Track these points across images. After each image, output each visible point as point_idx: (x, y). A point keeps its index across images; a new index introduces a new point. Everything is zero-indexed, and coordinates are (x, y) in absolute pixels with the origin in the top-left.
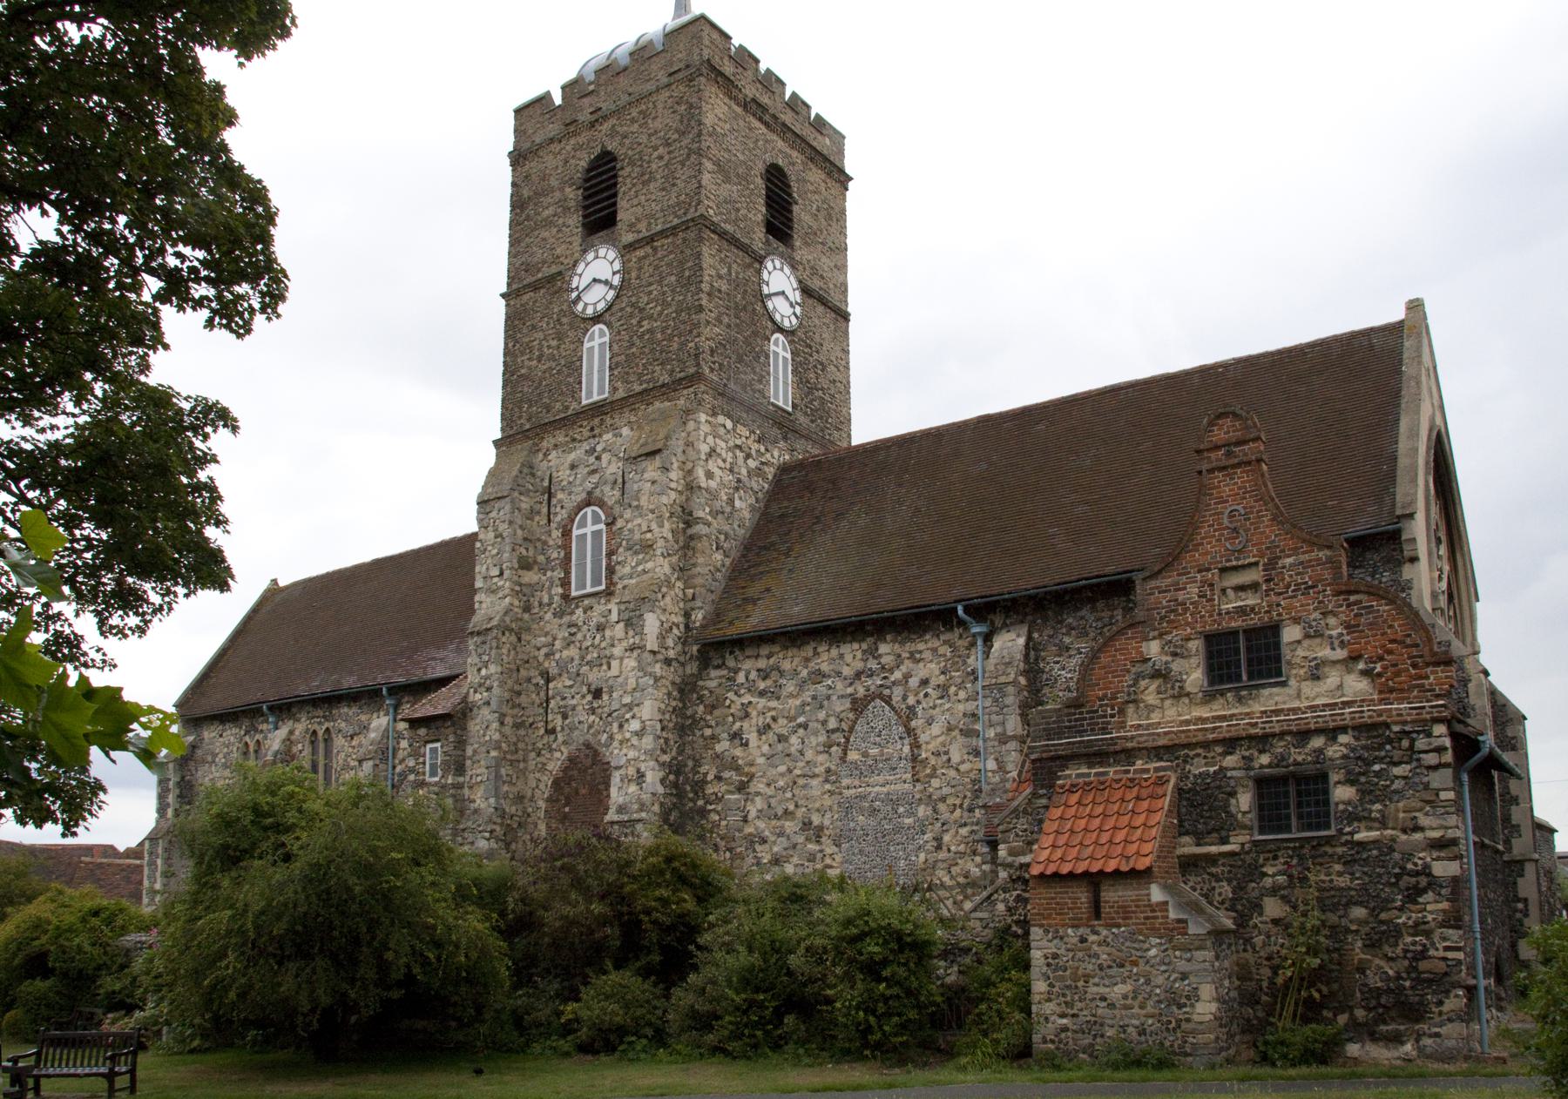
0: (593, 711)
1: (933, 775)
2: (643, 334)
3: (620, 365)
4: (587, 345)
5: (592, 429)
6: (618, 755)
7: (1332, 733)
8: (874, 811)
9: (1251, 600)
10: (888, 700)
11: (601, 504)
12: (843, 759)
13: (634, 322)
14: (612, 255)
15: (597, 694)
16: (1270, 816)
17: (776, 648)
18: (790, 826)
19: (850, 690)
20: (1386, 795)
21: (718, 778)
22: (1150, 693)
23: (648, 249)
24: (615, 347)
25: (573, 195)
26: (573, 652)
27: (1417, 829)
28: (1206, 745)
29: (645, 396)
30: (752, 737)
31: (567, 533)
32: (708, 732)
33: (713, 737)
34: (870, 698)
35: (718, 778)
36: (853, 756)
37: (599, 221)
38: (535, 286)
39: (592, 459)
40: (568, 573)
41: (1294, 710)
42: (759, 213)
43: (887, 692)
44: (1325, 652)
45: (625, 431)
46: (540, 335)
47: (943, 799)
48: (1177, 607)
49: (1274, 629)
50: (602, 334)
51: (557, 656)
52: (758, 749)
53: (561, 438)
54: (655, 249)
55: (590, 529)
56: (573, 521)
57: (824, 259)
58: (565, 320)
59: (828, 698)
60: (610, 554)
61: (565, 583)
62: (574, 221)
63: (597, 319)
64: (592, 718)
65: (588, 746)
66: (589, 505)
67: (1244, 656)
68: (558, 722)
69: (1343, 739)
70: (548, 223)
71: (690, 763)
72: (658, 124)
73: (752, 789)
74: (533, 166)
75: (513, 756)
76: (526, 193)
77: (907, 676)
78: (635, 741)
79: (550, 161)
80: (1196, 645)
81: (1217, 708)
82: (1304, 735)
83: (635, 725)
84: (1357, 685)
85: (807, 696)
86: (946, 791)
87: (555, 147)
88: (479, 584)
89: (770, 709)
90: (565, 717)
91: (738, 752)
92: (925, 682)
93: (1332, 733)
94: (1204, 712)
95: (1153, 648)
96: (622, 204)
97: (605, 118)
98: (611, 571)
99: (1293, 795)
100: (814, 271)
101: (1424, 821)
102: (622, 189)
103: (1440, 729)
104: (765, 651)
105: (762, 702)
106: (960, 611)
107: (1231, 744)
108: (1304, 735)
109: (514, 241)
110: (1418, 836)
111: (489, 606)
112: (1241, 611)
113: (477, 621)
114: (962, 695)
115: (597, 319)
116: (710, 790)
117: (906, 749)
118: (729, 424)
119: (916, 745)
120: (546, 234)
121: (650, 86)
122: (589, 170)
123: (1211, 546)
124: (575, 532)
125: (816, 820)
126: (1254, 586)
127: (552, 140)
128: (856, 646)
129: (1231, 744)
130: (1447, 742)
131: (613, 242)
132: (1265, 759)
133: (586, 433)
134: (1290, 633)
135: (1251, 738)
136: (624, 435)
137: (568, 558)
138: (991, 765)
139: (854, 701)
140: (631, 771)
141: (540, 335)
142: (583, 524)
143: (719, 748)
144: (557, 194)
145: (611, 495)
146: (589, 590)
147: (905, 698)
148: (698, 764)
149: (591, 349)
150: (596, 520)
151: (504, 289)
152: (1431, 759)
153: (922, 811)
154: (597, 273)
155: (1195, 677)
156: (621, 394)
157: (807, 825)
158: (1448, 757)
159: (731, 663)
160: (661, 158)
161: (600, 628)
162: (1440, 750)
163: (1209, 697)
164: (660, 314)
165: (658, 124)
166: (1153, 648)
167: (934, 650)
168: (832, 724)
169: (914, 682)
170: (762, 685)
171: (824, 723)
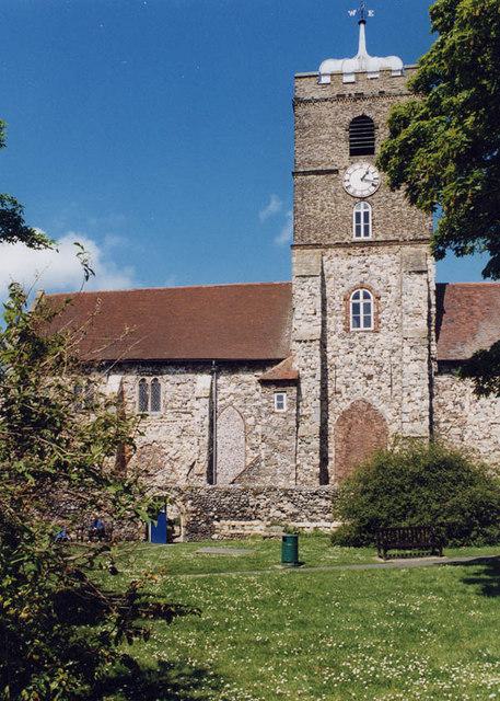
24: (376, 215)
30: (466, 404)
35: (448, 421)
51: (341, 357)
53: (340, 251)
62: (345, 146)
64: (366, 389)
68: (343, 388)
70: (323, 142)
122: (351, 123)
144: (331, 130)
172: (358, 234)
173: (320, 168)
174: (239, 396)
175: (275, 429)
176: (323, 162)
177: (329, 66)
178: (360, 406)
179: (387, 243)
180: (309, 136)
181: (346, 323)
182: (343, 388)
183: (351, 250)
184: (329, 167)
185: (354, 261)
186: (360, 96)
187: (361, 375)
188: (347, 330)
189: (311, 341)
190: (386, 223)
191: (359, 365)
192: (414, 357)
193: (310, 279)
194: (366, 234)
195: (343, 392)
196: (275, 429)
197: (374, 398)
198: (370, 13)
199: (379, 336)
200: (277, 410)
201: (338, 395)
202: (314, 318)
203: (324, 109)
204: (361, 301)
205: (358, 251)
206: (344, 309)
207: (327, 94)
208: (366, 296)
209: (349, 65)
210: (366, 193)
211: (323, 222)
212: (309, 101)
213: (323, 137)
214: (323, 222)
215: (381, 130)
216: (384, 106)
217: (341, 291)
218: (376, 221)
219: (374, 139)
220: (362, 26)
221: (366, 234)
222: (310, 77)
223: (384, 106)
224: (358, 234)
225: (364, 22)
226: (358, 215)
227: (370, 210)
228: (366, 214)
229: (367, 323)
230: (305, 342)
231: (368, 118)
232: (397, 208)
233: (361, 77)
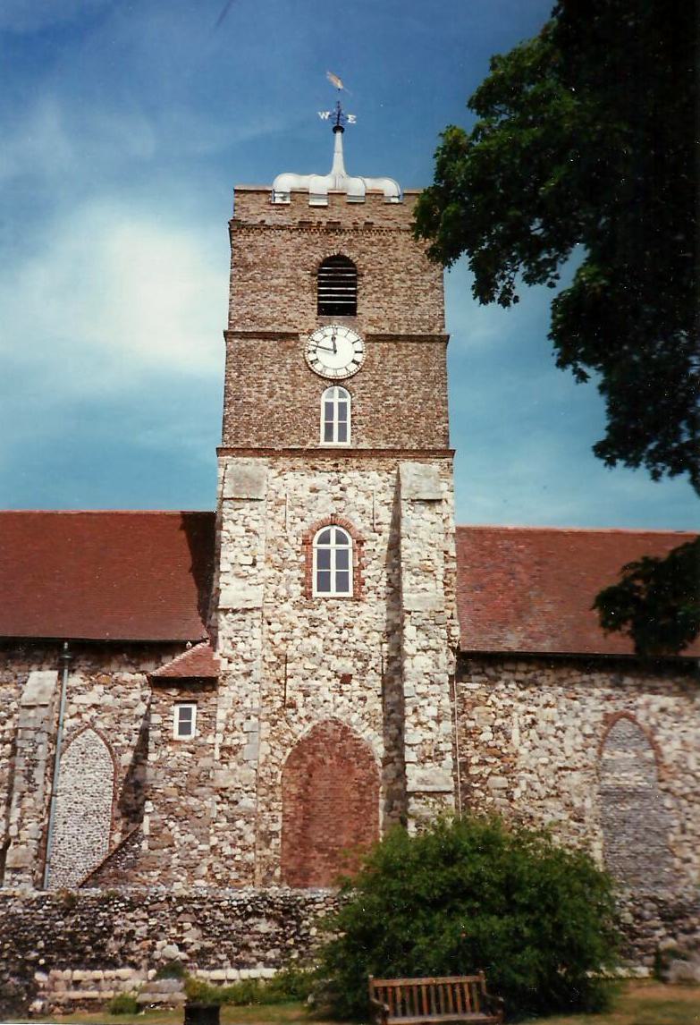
0: (341, 693)
2: (388, 407)
4: (324, 399)
5: (336, 465)
13: (379, 394)
19: (601, 707)
23: (392, 345)
24: (358, 409)
30: (515, 733)
35: (483, 763)
39: (336, 488)
40: (309, 575)
43: (632, 712)
51: (297, 642)
53: (299, 462)
54: (399, 348)
56: (314, 533)
59: (583, 710)
62: (309, 298)
64: (339, 699)
65: (336, 722)
66: (333, 524)
68: (300, 698)
70: (277, 290)
77: (648, 705)
78: (432, 724)
89: (529, 713)
90: (307, 695)
105: (522, 707)
115: (337, 382)
120: (277, 299)
122: (323, 265)
127: (282, 228)
128: (604, 675)
131: (353, 327)
139: (606, 715)
144: (289, 273)
147: (647, 719)
157: (569, 806)
164: (407, 396)
167: (669, 688)
168: (588, 730)
169: (654, 708)
170: (521, 694)
172: (329, 437)
173: (269, 329)
174: (109, 709)
175: (172, 773)
176: (274, 320)
177: (286, 182)
178: (329, 731)
179: (376, 453)
180: (253, 279)
181: (305, 583)
182: (300, 698)
183: (317, 462)
184: (285, 329)
185: (321, 480)
186: (334, 227)
187: (330, 674)
188: (307, 595)
189: (246, 610)
190: (375, 423)
191: (328, 658)
192: (425, 643)
193: (248, 505)
194: (342, 438)
195: (299, 704)
196: (172, 773)
197: (355, 718)
198: (351, 119)
199: (363, 607)
200: (176, 736)
201: (291, 711)
202: (252, 571)
203: (277, 241)
204: (333, 546)
205: (329, 464)
206: (302, 558)
207: (284, 220)
208: (341, 539)
209: (318, 184)
210: (342, 374)
211: (271, 415)
212: (255, 227)
213: (275, 282)
214: (271, 415)
216: (372, 244)
217: (298, 528)
218: (357, 418)
219: (355, 292)
220: (339, 135)
221: (342, 438)
222: (258, 192)
223: (372, 244)
224: (329, 437)
225: (342, 130)
226: (329, 406)
227: (348, 400)
228: (342, 406)
229: (342, 585)
230: (235, 612)
231: (347, 259)
232: (391, 400)
233: (337, 200)
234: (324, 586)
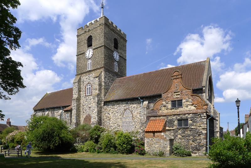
1: (135, 119)
3: (93, 65)
4: (88, 62)
6: (92, 115)
7: (189, 114)
8: (127, 123)
9: (179, 96)
10: (129, 109)
11: (90, 83)
12: (123, 116)
14: (91, 50)
15: (90, 108)
16: (180, 124)
17: (114, 102)
18: (115, 125)
20: (196, 122)
21: (106, 119)
22: (163, 108)
25: (86, 42)
26: (87, 102)
27: (200, 127)
28: (171, 115)
29: (96, 69)
30: (111, 114)
31: (86, 87)
32: (105, 113)
33: (105, 113)
34: (126, 109)
35: (106, 119)
36: (124, 116)
37: (90, 45)
38: (81, 54)
40: (86, 92)
41: (184, 111)
42: (113, 45)
44: (189, 103)
45: (94, 74)
46: (81, 61)
47: (136, 122)
48: (168, 97)
49: (182, 100)
50: (90, 61)
52: (111, 115)
53: (85, 74)
55: (89, 87)
57: (123, 52)
58: (85, 59)
60: (91, 90)
61: (85, 94)
62: (86, 45)
63: (90, 59)
67: (177, 104)
69: (190, 115)
70: (83, 46)
71: (102, 117)
72: (98, 32)
73: (110, 120)
74: (80, 37)
75: (78, 116)
76: (79, 41)
77: (132, 106)
78: (95, 114)
79: (82, 37)
80: (170, 102)
81: (173, 110)
82: (185, 114)
83: (95, 112)
84: (193, 108)
85: (118, 109)
86: (137, 121)
87: (83, 35)
88: (73, 94)
91: (109, 115)
92: (134, 107)
93: (189, 114)
94: (171, 111)
95: (164, 103)
96: (93, 43)
97: (90, 31)
98: (92, 92)
99: (183, 122)
100: (121, 54)
101: (201, 125)
102: (93, 41)
103: (205, 114)
104: (112, 103)
106: (139, 98)
107: (174, 115)
108: (185, 114)
109: (78, 48)
110: (201, 128)
111: (75, 96)
112: (177, 98)
113: (73, 98)
114: (139, 109)
115: (90, 59)
116: (105, 120)
117: (131, 115)
118: (108, 74)
119: (133, 115)
121: (97, 26)
122: (88, 38)
123: (173, 89)
124: (87, 87)
125: (119, 124)
126: (179, 95)
129: (174, 115)
130: (206, 116)
131: (92, 48)
132: (179, 117)
133: (88, 74)
134: (184, 101)
135: (177, 114)
136: (93, 74)
137: (86, 90)
138: (143, 117)
140: (94, 118)
141: (81, 61)
142: (88, 86)
143: (106, 115)
145: (91, 82)
146: (89, 95)
147: (131, 109)
148: (103, 117)
149: (89, 63)
150: (90, 86)
151: (76, 54)
152: (203, 118)
153: (133, 123)
154: (89, 53)
155: (170, 106)
156: (93, 69)
157: (118, 125)
158: (206, 118)
159: (108, 104)
160: (98, 37)
161: (90, 100)
162: (205, 116)
163: (171, 109)
165: (98, 32)
166: (164, 103)
167: (135, 103)
168: (122, 112)
169: (133, 107)
170: (112, 107)
171: (120, 112)
215: (94, 38)
220: (102, 9)
228: (90, 63)
234: (88, 94)
